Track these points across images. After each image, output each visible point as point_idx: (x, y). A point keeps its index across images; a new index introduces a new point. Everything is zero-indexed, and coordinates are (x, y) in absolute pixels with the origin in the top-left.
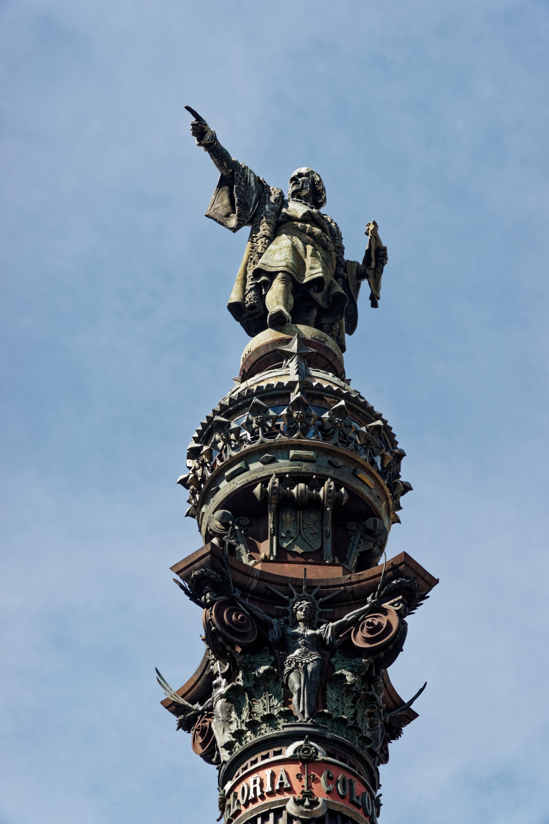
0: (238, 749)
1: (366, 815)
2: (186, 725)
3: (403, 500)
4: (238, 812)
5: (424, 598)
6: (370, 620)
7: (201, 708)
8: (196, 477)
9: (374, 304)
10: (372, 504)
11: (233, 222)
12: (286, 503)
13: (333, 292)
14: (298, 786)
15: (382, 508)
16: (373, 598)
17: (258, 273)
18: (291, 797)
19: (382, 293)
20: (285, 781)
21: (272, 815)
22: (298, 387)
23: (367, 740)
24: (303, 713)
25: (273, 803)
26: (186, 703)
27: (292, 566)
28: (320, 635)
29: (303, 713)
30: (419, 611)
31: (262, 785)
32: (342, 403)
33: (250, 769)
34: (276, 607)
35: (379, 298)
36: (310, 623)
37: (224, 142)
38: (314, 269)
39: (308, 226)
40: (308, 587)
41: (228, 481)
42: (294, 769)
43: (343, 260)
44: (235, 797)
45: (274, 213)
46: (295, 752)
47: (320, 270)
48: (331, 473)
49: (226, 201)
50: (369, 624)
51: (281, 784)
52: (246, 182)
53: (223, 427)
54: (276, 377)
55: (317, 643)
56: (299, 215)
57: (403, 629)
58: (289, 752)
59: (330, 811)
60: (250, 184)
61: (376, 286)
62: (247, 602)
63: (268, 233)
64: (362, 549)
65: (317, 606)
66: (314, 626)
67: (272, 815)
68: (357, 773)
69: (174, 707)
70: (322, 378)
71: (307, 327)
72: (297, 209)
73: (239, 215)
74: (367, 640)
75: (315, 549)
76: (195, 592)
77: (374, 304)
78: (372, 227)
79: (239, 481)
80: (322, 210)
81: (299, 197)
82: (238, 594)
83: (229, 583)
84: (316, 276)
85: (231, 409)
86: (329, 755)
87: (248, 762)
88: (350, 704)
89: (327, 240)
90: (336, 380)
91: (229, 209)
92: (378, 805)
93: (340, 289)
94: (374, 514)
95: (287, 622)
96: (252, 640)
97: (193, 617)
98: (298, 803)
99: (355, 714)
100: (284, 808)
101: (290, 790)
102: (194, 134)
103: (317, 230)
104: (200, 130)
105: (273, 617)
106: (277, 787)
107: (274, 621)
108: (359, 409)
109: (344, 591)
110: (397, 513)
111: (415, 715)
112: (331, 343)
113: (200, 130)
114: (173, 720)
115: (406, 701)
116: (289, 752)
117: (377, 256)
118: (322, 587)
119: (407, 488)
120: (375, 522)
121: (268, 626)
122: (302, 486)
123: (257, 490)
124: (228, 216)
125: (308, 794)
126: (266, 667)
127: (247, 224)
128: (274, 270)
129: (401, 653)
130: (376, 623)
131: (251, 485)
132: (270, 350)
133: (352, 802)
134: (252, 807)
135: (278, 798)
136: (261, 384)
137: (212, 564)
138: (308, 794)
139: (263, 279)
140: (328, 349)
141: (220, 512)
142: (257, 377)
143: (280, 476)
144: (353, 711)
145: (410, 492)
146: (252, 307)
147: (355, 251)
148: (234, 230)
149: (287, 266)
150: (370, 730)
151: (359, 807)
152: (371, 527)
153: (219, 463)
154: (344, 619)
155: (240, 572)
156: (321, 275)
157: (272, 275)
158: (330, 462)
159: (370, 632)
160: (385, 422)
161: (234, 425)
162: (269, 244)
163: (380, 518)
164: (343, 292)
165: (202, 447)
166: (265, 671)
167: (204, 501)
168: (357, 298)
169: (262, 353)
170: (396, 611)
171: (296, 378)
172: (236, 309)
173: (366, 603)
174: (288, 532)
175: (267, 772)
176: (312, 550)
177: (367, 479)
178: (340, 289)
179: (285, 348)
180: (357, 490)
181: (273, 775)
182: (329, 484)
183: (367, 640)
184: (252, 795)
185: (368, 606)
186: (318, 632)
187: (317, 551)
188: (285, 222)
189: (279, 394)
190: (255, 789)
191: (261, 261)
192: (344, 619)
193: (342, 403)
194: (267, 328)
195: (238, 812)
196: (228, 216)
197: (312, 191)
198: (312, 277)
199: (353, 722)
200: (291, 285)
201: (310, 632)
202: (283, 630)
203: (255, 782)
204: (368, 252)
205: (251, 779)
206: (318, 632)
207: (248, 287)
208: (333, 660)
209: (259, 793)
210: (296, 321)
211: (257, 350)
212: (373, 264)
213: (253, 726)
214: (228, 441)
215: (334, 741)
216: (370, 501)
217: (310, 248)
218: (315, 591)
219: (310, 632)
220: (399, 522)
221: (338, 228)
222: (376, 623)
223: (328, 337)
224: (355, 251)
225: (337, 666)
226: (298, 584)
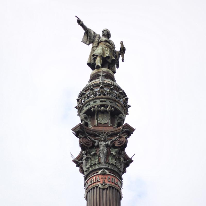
0: (88, 172)
1: (119, 186)
2: (78, 166)
3: (129, 109)
4: (88, 187)
5: (132, 133)
6: (119, 140)
7: (81, 162)
8: (79, 106)
9: (123, 61)
10: (120, 111)
11: (88, 43)
12: (99, 112)
13: (112, 59)
14: (102, 181)
15: (123, 112)
16: (120, 134)
17: (94, 55)
18: (100, 183)
19: (125, 58)
20: (99, 179)
21: (96, 188)
22: (101, 83)
23: (119, 169)
24: (103, 163)
25: (96, 185)
26: (78, 161)
27: (101, 127)
28: (107, 144)
29: (103, 163)
30: (131, 137)
31: (93, 180)
32: (112, 87)
33: (91, 177)
34: (97, 137)
35: (124, 60)
36: (105, 141)
37: (85, 24)
38: (107, 54)
39: (106, 43)
40: (104, 132)
41: (86, 107)
42: (101, 176)
43: (115, 50)
44: (87, 183)
45: (98, 40)
46: (101, 172)
47: (109, 54)
48: (110, 104)
49: (86, 38)
50: (118, 141)
51: (98, 180)
52: (91, 33)
53: (84, 94)
54: (97, 81)
55: (107, 146)
56: (104, 40)
57: (126, 143)
58: (100, 172)
60: (92, 33)
61: (123, 57)
62: (89, 137)
63: (96, 45)
64: (118, 122)
65: (106, 137)
66: (106, 142)
67: (96, 188)
68: (116, 177)
69: (74, 161)
70: (108, 81)
71: (105, 68)
72: (104, 39)
73: (89, 41)
74: (118, 145)
75: (107, 123)
76: (77, 135)
77: (123, 61)
78: (121, 43)
80: (110, 39)
81: (104, 36)
82: (87, 134)
83: (85, 132)
84: (107, 55)
85: (86, 90)
86: (109, 173)
87: (90, 175)
88: (115, 160)
89: (111, 46)
90: (111, 81)
91: (87, 40)
92: (122, 184)
93: (114, 58)
94: (121, 113)
95: (99, 141)
96: (91, 146)
97: (76, 140)
98: (102, 184)
99: (116, 162)
100: (98, 186)
101: (99, 181)
102: (78, 22)
103: (108, 44)
104: (79, 21)
105: (96, 140)
106: (97, 181)
108: (118, 88)
109: (113, 133)
110: (128, 112)
112: (111, 72)
113: (79, 21)
114: (75, 165)
115: (130, 157)
116: (100, 172)
117: (123, 50)
118: (107, 132)
119: (129, 106)
120: (121, 115)
121: (95, 142)
122: (103, 108)
123: (92, 109)
124: (87, 41)
125: (104, 182)
126: (94, 152)
127: (91, 43)
128: (97, 54)
129: (127, 147)
130: (120, 140)
131: (91, 108)
132: (96, 74)
133: (115, 184)
134: (91, 186)
135: (97, 183)
136: (93, 83)
137: (81, 128)
138: (104, 182)
139: (94, 57)
140: (110, 74)
141: (84, 115)
142: (93, 81)
143: (98, 106)
144: (115, 162)
145: (130, 107)
146: (92, 64)
147: (118, 48)
148: (88, 45)
149: (100, 53)
150: (120, 166)
151: (116, 185)
152: (120, 117)
153: (83, 103)
154: (113, 140)
155: (88, 129)
156: (109, 55)
157: (97, 56)
158: (110, 102)
159: (119, 142)
160: (123, 91)
161: (86, 94)
162: (96, 48)
163: (122, 114)
164: (114, 59)
165: (79, 99)
166: (94, 153)
167: (80, 112)
168: (119, 59)
169: (94, 75)
170: (125, 137)
171: (101, 81)
172: (89, 64)
173: (118, 135)
174: (100, 119)
175: (95, 177)
176: (106, 123)
178: (114, 58)
179: (100, 74)
180: (116, 108)
181: (96, 178)
182: (109, 107)
183: (118, 145)
184: (91, 183)
185: (118, 136)
186: (106, 143)
187: (107, 123)
188: (100, 42)
189: (97, 85)
190: (92, 181)
191: (94, 52)
192: (113, 140)
193: (112, 87)
194: (95, 69)
195: (88, 187)
196: (87, 41)
197: (107, 34)
198: (107, 56)
199: (115, 164)
200: (101, 58)
201: (105, 143)
202: (98, 143)
203: (92, 180)
204: (121, 49)
205: (91, 179)
206: (106, 143)
207: (92, 59)
208: (110, 150)
209: (93, 183)
210: (102, 67)
211: (93, 74)
212: (122, 51)
213: (91, 166)
214: (85, 97)
216: (120, 110)
217: (106, 48)
218: (106, 133)
219: (105, 143)
220: (128, 114)
221: (114, 43)
222: (120, 140)
223: (110, 70)
224: (118, 48)
225: (111, 151)
226: (102, 132)
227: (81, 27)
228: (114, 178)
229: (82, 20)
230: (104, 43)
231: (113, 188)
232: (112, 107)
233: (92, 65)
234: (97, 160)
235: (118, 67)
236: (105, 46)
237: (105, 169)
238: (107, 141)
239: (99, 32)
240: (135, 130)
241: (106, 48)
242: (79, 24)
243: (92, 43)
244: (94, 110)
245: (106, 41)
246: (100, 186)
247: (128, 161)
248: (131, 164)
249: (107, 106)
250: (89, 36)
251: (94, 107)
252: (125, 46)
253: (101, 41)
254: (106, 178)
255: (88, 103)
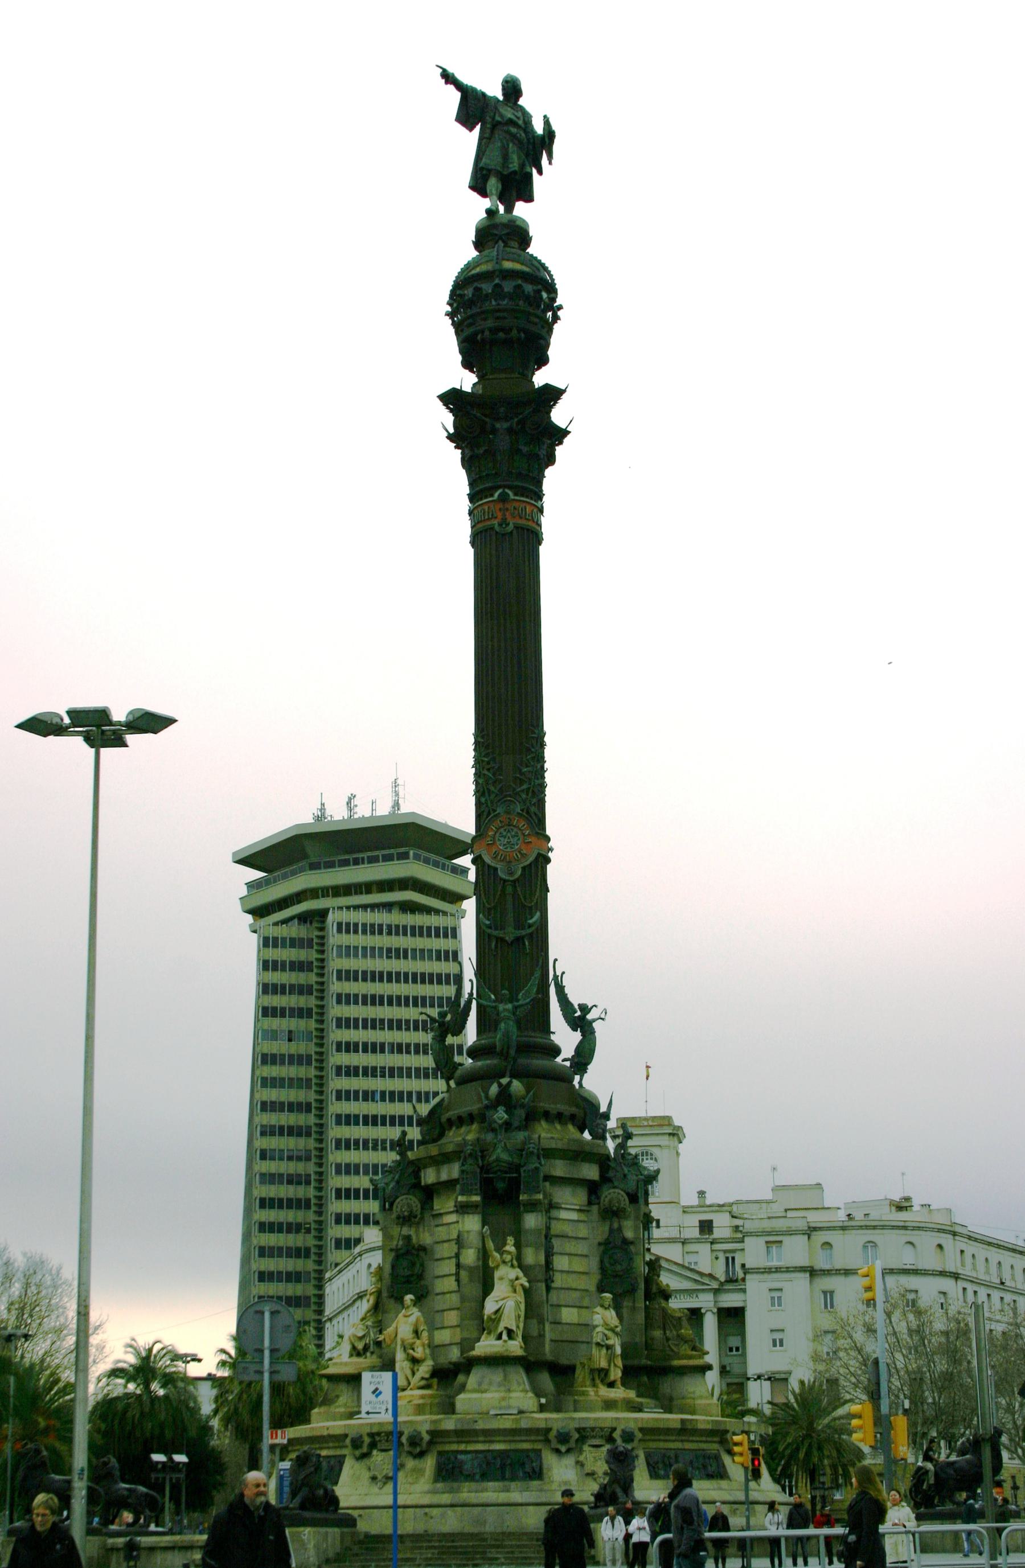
3: (560, 313)
9: (550, 163)
14: (499, 515)
15: (544, 332)
17: (482, 169)
18: (496, 522)
22: (497, 273)
46: (499, 495)
58: (496, 495)
59: (516, 527)
77: (550, 163)
79: (471, 330)
80: (522, 102)
92: (541, 511)
103: (514, 130)
107: (487, 420)
111: (569, 432)
116: (496, 495)
117: (550, 135)
119: (560, 308)
123: (479, 337)
131: (475, 334)
143: (490, 330)
157: (489, 171)
172: (473, 187)
177: (536, 320)
182: (514, 332)
201: (506, 425)
215: (517, 487)
219: (506, 425)
224: (539, 128)
227: (451, 87)
228: (522, 505)
229: (450, 70)
230: (505, 128)
231: (523, 529)
232: (519, 330)
233: (478, 186)
234: (491, 465)
235: (540, 172)
236: (508, 137)
237: (505, 487)
238: (512, 418)
239: (495, 91)
240: (564, 391)
241: (511, 145)
242: (447, 83)
243: (481, 119)
244: (483, 340)
245: (511, 122)
246: (496, 527)
247: (560, 435)
248: (565, 440)
249: (511, 330)
250: (473, 108)
251: (483, 332)
252: (554, 128)
253: (499, 123)
254: (507, 509)
255: (470, 321)
